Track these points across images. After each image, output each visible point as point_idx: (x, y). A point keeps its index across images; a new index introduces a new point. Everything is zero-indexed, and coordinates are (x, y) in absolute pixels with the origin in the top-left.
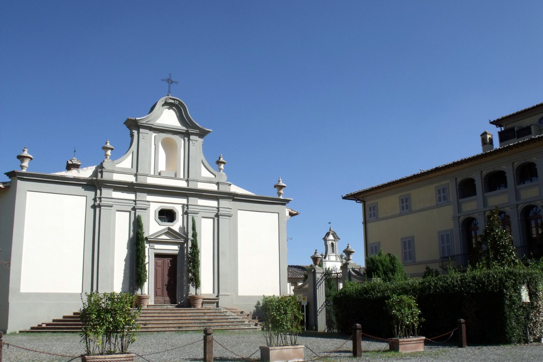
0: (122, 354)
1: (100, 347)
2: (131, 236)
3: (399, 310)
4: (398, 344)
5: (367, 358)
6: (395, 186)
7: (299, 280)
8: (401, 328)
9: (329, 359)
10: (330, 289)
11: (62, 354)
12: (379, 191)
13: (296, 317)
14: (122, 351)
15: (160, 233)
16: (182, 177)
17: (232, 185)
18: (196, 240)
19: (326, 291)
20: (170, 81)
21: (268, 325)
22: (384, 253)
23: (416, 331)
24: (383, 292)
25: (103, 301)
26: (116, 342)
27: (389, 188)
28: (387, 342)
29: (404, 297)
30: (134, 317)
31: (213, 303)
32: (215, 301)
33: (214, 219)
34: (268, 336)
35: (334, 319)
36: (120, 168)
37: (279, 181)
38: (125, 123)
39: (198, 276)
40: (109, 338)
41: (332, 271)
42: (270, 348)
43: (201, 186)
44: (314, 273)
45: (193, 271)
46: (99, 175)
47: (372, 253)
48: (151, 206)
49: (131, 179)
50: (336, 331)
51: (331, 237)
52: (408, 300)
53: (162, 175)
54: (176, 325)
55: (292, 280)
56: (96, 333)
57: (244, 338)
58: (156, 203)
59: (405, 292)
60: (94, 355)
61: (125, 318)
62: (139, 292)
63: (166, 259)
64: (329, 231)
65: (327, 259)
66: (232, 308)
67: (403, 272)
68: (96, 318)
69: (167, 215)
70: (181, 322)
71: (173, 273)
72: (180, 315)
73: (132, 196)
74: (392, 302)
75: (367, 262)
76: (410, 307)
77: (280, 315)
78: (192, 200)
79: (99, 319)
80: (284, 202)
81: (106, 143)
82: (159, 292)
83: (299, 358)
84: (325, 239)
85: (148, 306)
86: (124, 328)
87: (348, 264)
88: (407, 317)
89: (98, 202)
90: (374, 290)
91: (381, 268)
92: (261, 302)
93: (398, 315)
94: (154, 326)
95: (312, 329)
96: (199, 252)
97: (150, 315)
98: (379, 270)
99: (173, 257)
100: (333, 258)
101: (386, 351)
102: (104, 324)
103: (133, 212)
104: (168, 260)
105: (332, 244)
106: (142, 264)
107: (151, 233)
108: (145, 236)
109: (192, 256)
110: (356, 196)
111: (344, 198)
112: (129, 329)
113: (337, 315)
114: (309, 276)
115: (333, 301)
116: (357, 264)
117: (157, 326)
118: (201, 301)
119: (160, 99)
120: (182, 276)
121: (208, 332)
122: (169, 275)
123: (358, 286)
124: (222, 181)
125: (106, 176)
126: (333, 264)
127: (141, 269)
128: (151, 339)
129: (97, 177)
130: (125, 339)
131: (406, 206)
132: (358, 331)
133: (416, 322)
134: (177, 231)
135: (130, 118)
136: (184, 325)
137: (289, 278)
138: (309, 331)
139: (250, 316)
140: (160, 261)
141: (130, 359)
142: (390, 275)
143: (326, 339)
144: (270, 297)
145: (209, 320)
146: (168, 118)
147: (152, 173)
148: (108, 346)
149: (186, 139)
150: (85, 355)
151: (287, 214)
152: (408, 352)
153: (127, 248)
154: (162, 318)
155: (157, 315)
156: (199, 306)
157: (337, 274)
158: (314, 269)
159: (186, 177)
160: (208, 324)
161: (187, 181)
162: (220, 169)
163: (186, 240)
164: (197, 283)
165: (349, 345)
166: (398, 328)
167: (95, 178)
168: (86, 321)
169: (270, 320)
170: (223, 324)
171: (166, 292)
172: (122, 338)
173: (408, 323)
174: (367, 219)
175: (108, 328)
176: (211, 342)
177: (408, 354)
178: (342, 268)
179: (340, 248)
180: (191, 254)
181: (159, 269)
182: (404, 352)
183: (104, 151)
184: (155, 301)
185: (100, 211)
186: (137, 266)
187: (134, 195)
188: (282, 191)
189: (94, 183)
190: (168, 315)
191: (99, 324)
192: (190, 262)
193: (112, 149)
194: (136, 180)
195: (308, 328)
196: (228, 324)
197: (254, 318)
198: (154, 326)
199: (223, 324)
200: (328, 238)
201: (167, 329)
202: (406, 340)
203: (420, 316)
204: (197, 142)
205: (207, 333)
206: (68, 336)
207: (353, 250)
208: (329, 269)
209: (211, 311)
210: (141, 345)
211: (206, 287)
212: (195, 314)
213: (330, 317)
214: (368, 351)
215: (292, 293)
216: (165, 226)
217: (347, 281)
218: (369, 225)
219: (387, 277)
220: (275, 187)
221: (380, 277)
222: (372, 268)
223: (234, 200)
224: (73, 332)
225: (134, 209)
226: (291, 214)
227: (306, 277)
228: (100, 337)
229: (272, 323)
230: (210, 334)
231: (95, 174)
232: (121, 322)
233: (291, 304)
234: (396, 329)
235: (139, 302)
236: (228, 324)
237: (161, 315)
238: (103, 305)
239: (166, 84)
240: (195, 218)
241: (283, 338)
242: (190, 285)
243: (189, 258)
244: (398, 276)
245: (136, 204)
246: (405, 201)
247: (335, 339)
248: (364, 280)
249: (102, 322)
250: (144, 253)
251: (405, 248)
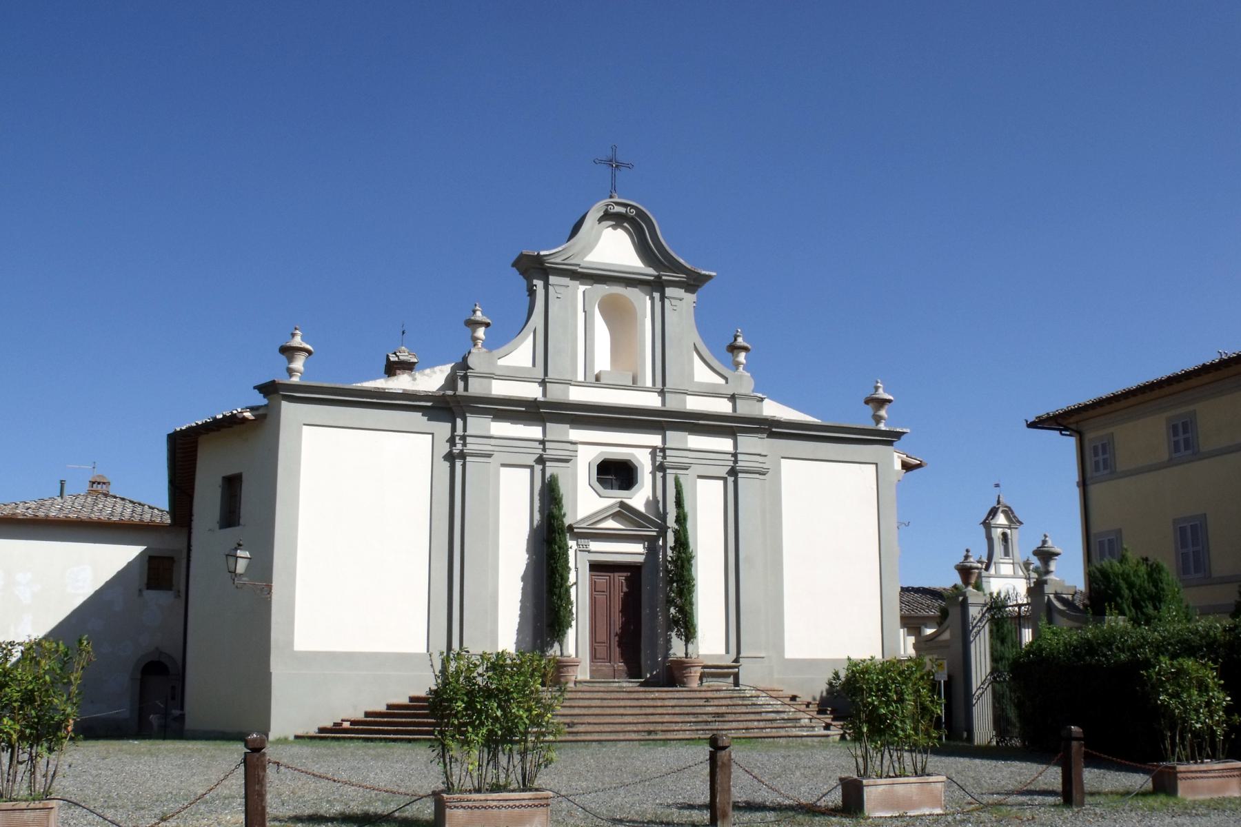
0: (523, 791)
1: (475, 774)
2: (535, 523)
3: (1176, 695)
4: (1176, 778)
5: (1098, 811)
6: (1157, 393)
7: (926, 621)
8: (1182, 738)
9: (1004, 809)
10: (1003, 641)
11: (389, 788)
12: (1116, 405)
13: (924, 709)
14: (524, 784)
15: (601, 516)
16: (649, 383)
17: (766, 401)
18: (685, 530)
19: (992, 647)
20: (614, 164)
21: (860, 728)
22: (1133, 556)
23: (1220, 746)
24: (1133, 649)
25: (480, 670)
26: (509, 764)
27: (1140, 398)
28: (1145, 772)
29: (1189, 663)
30: (549, 708)
31: (726, 676)
32: (730, 672)
33: (725, 479)
34: (859, 753)
35: (1012, 713)
36: (508, 367)
37: (877, 388)
38: (513, 265)
39: (692, 614)
40: (495, 756)
41: (1008, 597)
42: (865, 782)
43: (694, 404)
44: (964, 605)
45: (678, 601)
46: (461, 384)
47: (1102, 557)
48: (579, 454)
49: (532, 391)
50: (1017, 742)
51: (1001, 519)
52: (1197, 671)
53: (603, 381)
54: (640, 727)
55: (911, 623)
56: (467, 742)
57: (800, 757)
58: (590, 447)
59: (1188, 649)
60: (461, 792)
61: (529, 710)
62: (555, 651)
63: (616, 574)
64: (995, 504)
65: (992, 571)
66: (769, 687)
67: (1181, 601)
68: (465, 709)
69: (616, 473)
70: (652, 719)
71: (632, 605)
72: (651, 703)
73: (535, 432)
74: (1158, 673)
75: (1090, 578)
76: (1203, 687)
77: (888, 704)
78: (674, 438)
79: (464, 710)
80: (890, 438)
81: (474, 312)
82: (602, 651)
83: (934, 807)
84: (987, 525)
85: (576, 683)
86: (526, 733)
87: (1045, 582)
88: (1197, 711)
89: (459, 447)
90: (1111, 644)
91: (1126, 592)
92: (843, 674)
93: (1173, 706)
94: (590, 728)
95: (961, 739)
96: (692, 557)
97: (581, 703)
98: (1122, 598)
99: (632, 571)
100: (1006, 569)
101: (1144, 794)
102: (482, 724)
103: (538, 468)
104: (620, 578)
105: (1005, 535)
106: (562, 586)
107: (581, 514)
108: (567, 521)
109: (676, 566)
110: (1060, 420)
111: (1032, 425)
112: (538, 735)
113: (1019, 706)
114: (951, 611)
115: (1011, 671)
116: (1067, 584)
117: (597, 728)
118: (699, 671)
119: (593, 205)
120: (654, 613)
121: (720, 744)
122: (624, 611)
123: (1070, 637)
124: (743, 392)
125: (476, 387)
126: (1008, 582)
127: (560, 598)
128: (586, 758)
129: (455, 388)
130: (529, 757)
131: (1184, 441)
132: (1075, 743)
133: (1218, 724)
134: (642, 509)
135: (525, 252)
136: (660, 727)
137: (903, 618)
138: (952, 743)
139: (813, 707)
140: (602, 579)
141: (542, 802)
142: (1150, 610)
143: (994, 763)
144: (864, 661)
145: (718, 715)
146: (613, 249)
147: (581, 378)
148: (491, 771)
149: (657, 295)
150: (443, 791)
151: (898, 466)
152: (1201, 797)
153: (528, 551)
154: (608, 711)
155: (598, 703)
156: (695, 684)
157: (1020, 606)
158: (964, 595)
159: (659, 385)
160: (716, 726)
161: (662, 393)
162: (737, 364)
163: (663, 531)
164: (688, 630)
165: (1052, 776)
166: (1173, 738)
167: (450, 393)
168: (442, 717)
169: (863, 716)
170: (750, 725)
171: (617, 651)
172: (523, 754)
173: (1198, 726)
174: (1089, 474)
175: (491, 732)
176: (727, 765)
177: (1202, 803)
178: (1030, 591)
179: (1024, 543)
180: (673, 562)
181: (601, 598)
182: (1190, 798)
183: (468, 330)
184: (591, 671)
185: (464, 466)
186: (551, 592)
187: (540, 429)
188: (883, 413)
189: (448, 403)
190: (622, 703)
191: (472, 724)
192: (671, 581)
193: (487, 325)
194: (544, 394)
195: (953, 737)
196: (762, 724)
197: (821, 711)
198: (590, 728)
199: (750, 725)
200: (993, 522)
201: (621, 737)
202: (1194, 767)
203: (1228, 710)
204: (682, 303)
205: (716, 746)
206: (399, 749)
207: (1057, 550)
208: (999, 594)
209: (722, 694)
210: (566, 772)
211: (710, 640)
212: (685, 702)
213: (1003, 710)
214: (1099, 793)
215: (911, 652)
216: (611, 499)
217: (1043, 623)
218: (1094, 489)
219: (1143, 613)
220: (867, 402)
221: (1124, 614)
222: (1103, 591)
223: (772, 435)
224: (409, 741)
225: (541, 460)
226: (907, 467)
227: (944, 614)
228: (475, 753)
229: (868, 722)
230: (724, 748)
231: (451, 382)
232: (521, 718)
233: (913, 677)
234: (1168, 742)
235: (557, 672)
236: (762, 724)
237: (606, 703)
238: (479, 680)
239: (606, 171)
240: (682, 480)
241: (895, 758)
242: (673, 634)
243: (670, 572)
244: (1170, 611)
245: (544, 450)
246: (1181, 429)
247: (1017, 763)
248: (1086, 622)
249: (479, 718)
250: (567, 561)
251: (1184, 544)
